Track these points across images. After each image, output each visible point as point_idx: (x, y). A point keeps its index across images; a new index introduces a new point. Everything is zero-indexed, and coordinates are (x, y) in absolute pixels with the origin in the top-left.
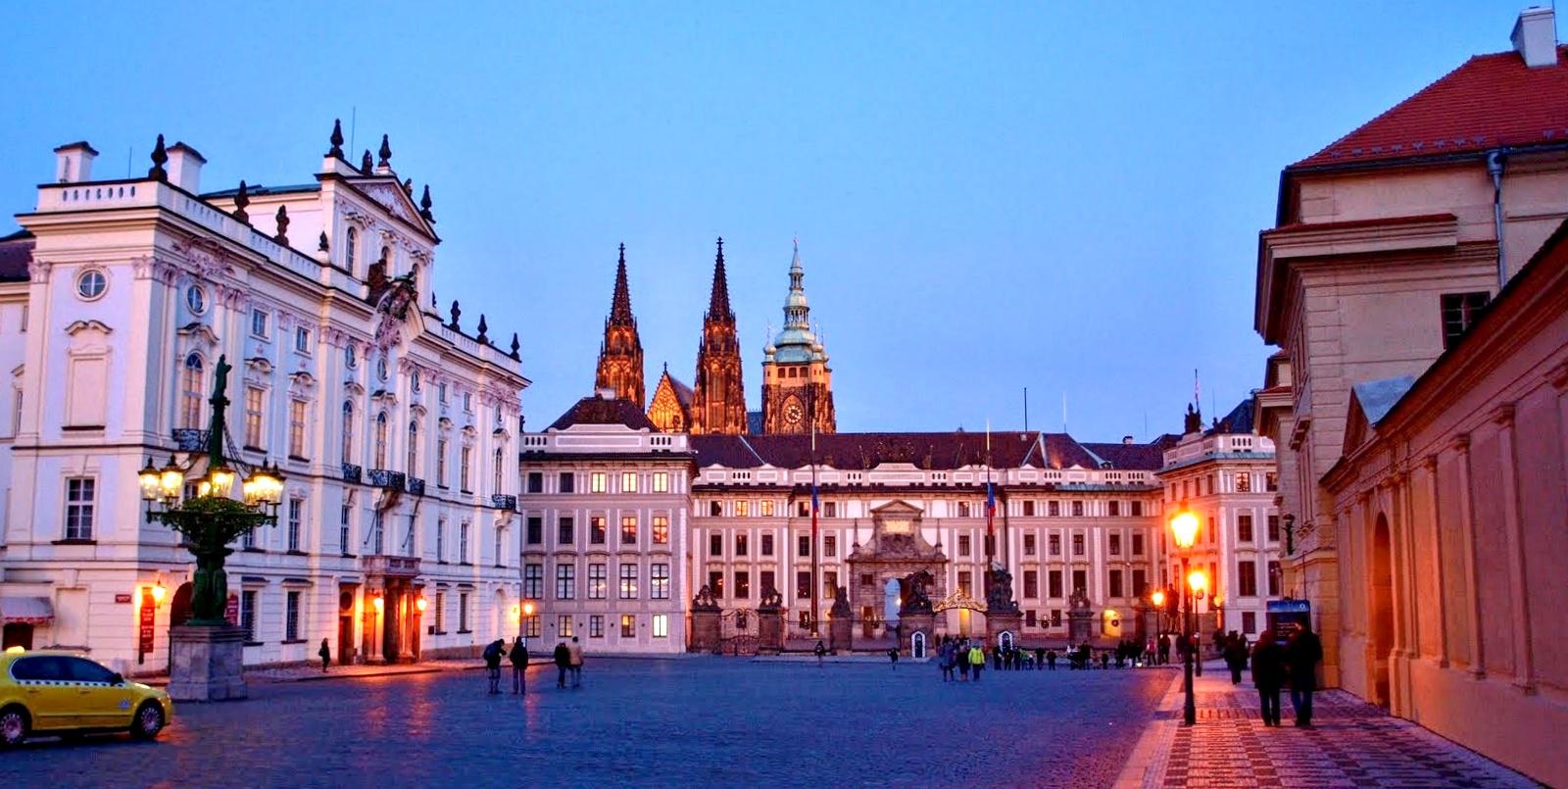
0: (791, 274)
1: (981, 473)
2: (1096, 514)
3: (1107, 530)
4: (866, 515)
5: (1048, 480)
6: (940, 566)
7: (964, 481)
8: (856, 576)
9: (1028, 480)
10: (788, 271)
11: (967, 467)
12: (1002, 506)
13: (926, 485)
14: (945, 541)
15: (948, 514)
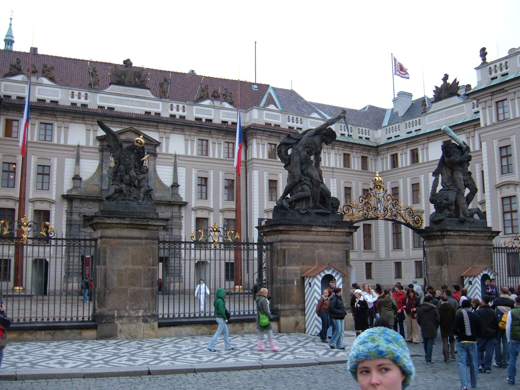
0: (5, 40)
1: (221, 111)
2: (332, 165)
3: (342, 182)
4: (91, 144)
5: (291, 124)
6: (176, 209)
7: (204, 117)
8: (76, 217)
9: (273, 122)
10: (4, 38)
11: (207, 102)
12: (245, 148)
13: (162, 115)
14: (182, 181)
15: (186, 151)
